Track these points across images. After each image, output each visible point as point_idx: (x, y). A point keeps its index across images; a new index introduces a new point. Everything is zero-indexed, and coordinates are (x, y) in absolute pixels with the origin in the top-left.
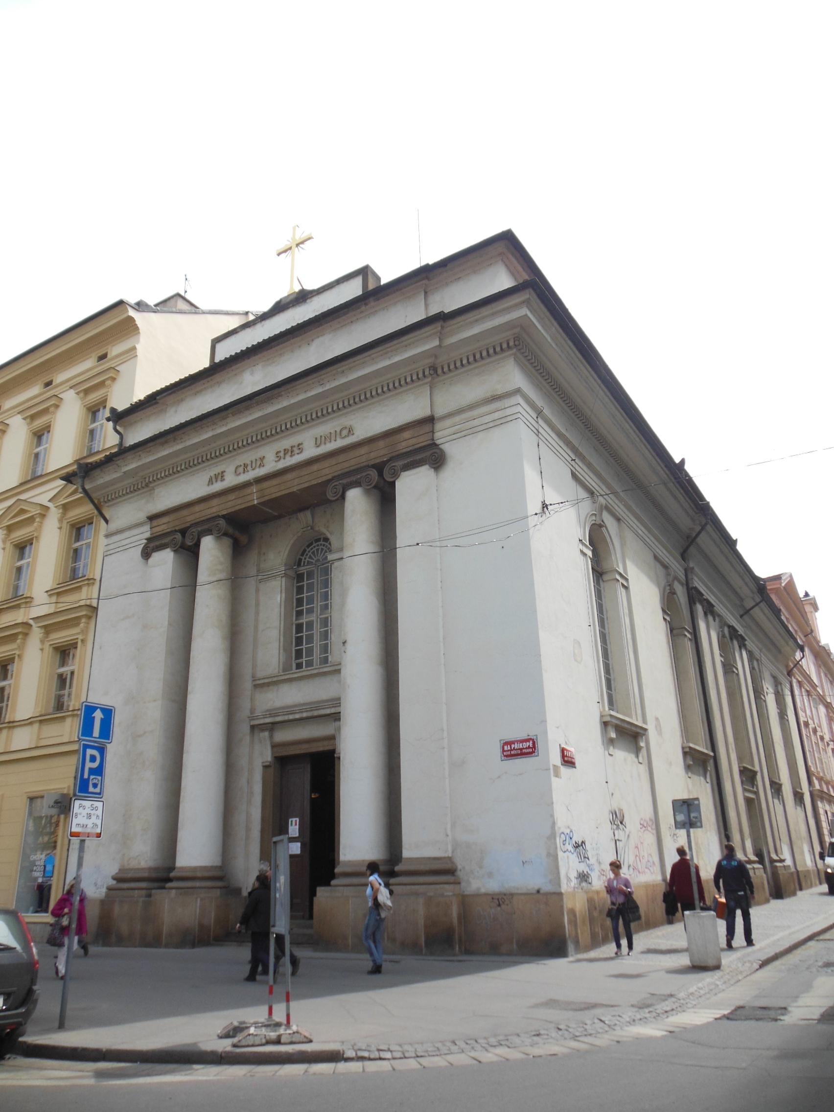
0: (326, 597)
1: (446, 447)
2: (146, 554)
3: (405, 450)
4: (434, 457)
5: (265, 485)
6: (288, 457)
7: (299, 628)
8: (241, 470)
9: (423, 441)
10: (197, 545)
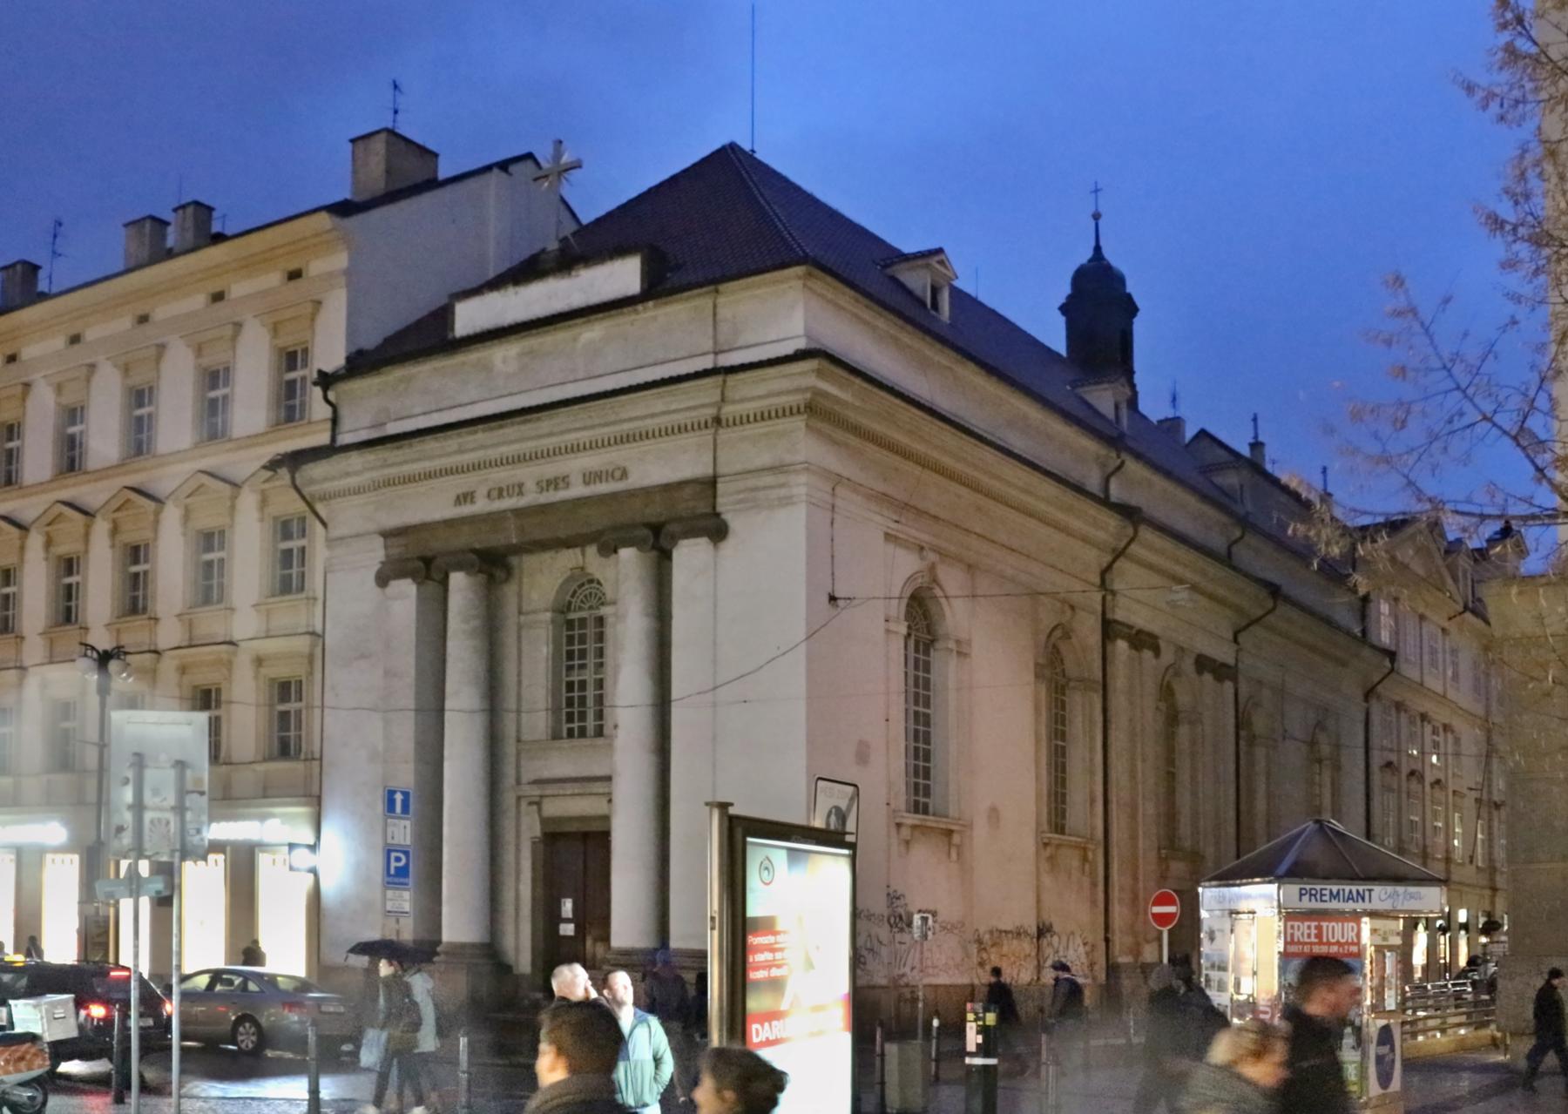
0: (600, 653)
1: (727, 517)
2: (382, 580)
4: (717, 531)
6: (551, 492)
7: (570, 686)
8: (495, 494)
9: (703, 508)
10: (446, 577)
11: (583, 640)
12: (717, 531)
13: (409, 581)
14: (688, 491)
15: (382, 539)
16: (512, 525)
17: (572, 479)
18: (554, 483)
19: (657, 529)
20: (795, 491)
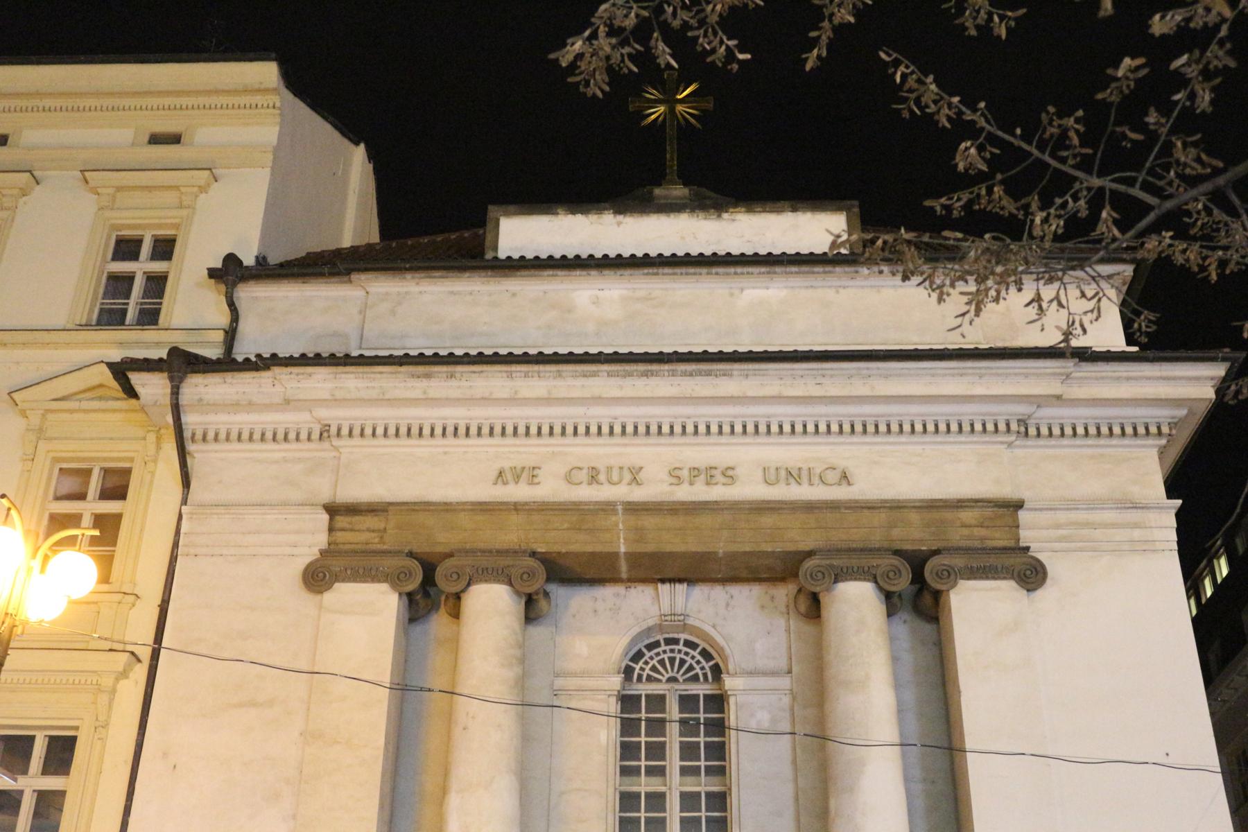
3: (963, 543)
5: (649, 522)
8: (583, 476)
11: (657, 726)
12: (1031, 575)
13: (384, 587)
14: (967, 516)
15: (326, 517)
16: (620, 520)
17: (739, 471)
18: (709, 474)
19: (917, 562)
20: (1157, 534)
